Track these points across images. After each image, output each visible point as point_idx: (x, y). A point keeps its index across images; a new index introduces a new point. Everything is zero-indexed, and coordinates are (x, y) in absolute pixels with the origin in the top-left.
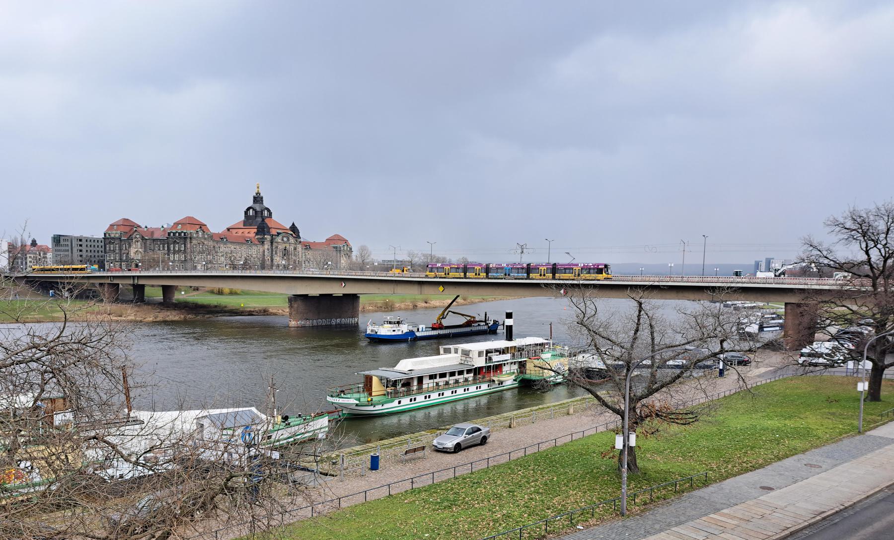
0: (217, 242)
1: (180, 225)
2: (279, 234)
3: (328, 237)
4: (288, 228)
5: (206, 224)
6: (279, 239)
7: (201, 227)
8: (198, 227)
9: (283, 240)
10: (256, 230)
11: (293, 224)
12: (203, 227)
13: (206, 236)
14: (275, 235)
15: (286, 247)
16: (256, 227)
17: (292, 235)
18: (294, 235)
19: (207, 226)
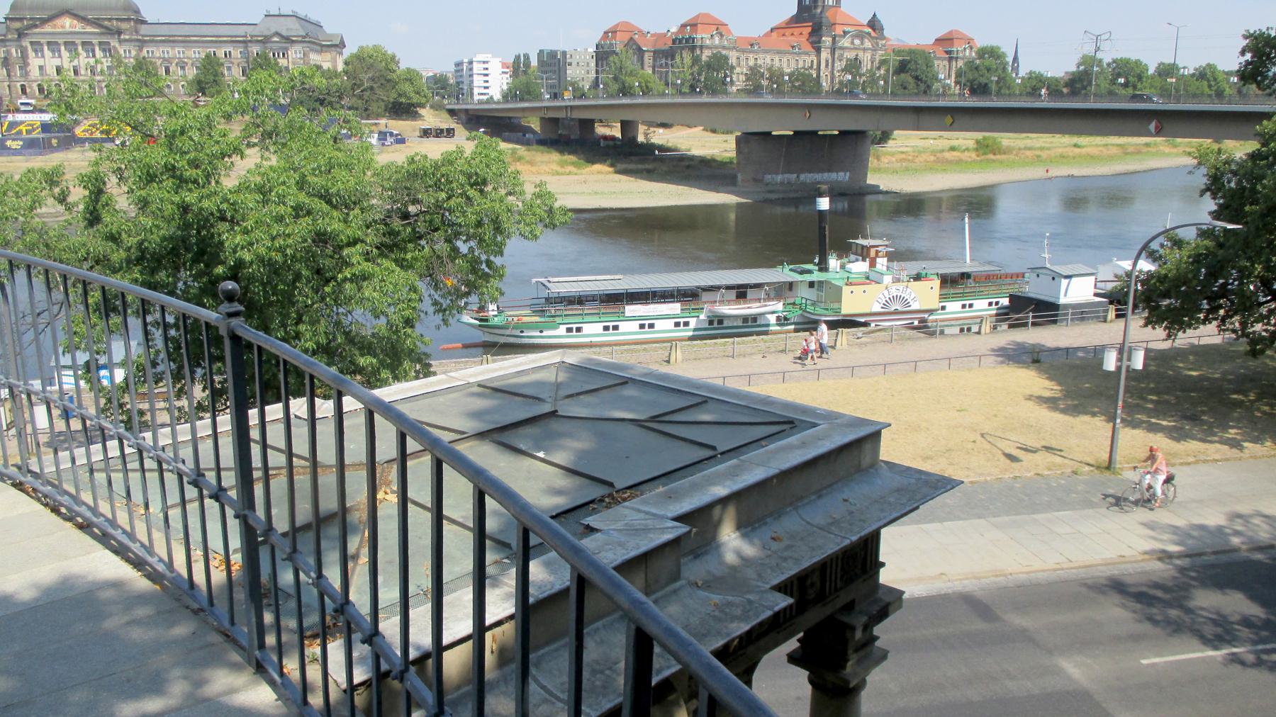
0: (743, 51)
1: (688, 28)
2: (845, 33)
3: (938, 35)
4: (865, 22)
5: (726, 22)
6: (845, 42)
7: (717, 29)
8: (714, 27)
9: (852, 43)
10: (809, 30)
11: (875, 15)
12: (722, 29)
13: (726, 43)
14: (841, 36)
15: (857, 55)
16: (811, 24)
17: (869, 34)
18: (873, 34)
19: (730, 26)
